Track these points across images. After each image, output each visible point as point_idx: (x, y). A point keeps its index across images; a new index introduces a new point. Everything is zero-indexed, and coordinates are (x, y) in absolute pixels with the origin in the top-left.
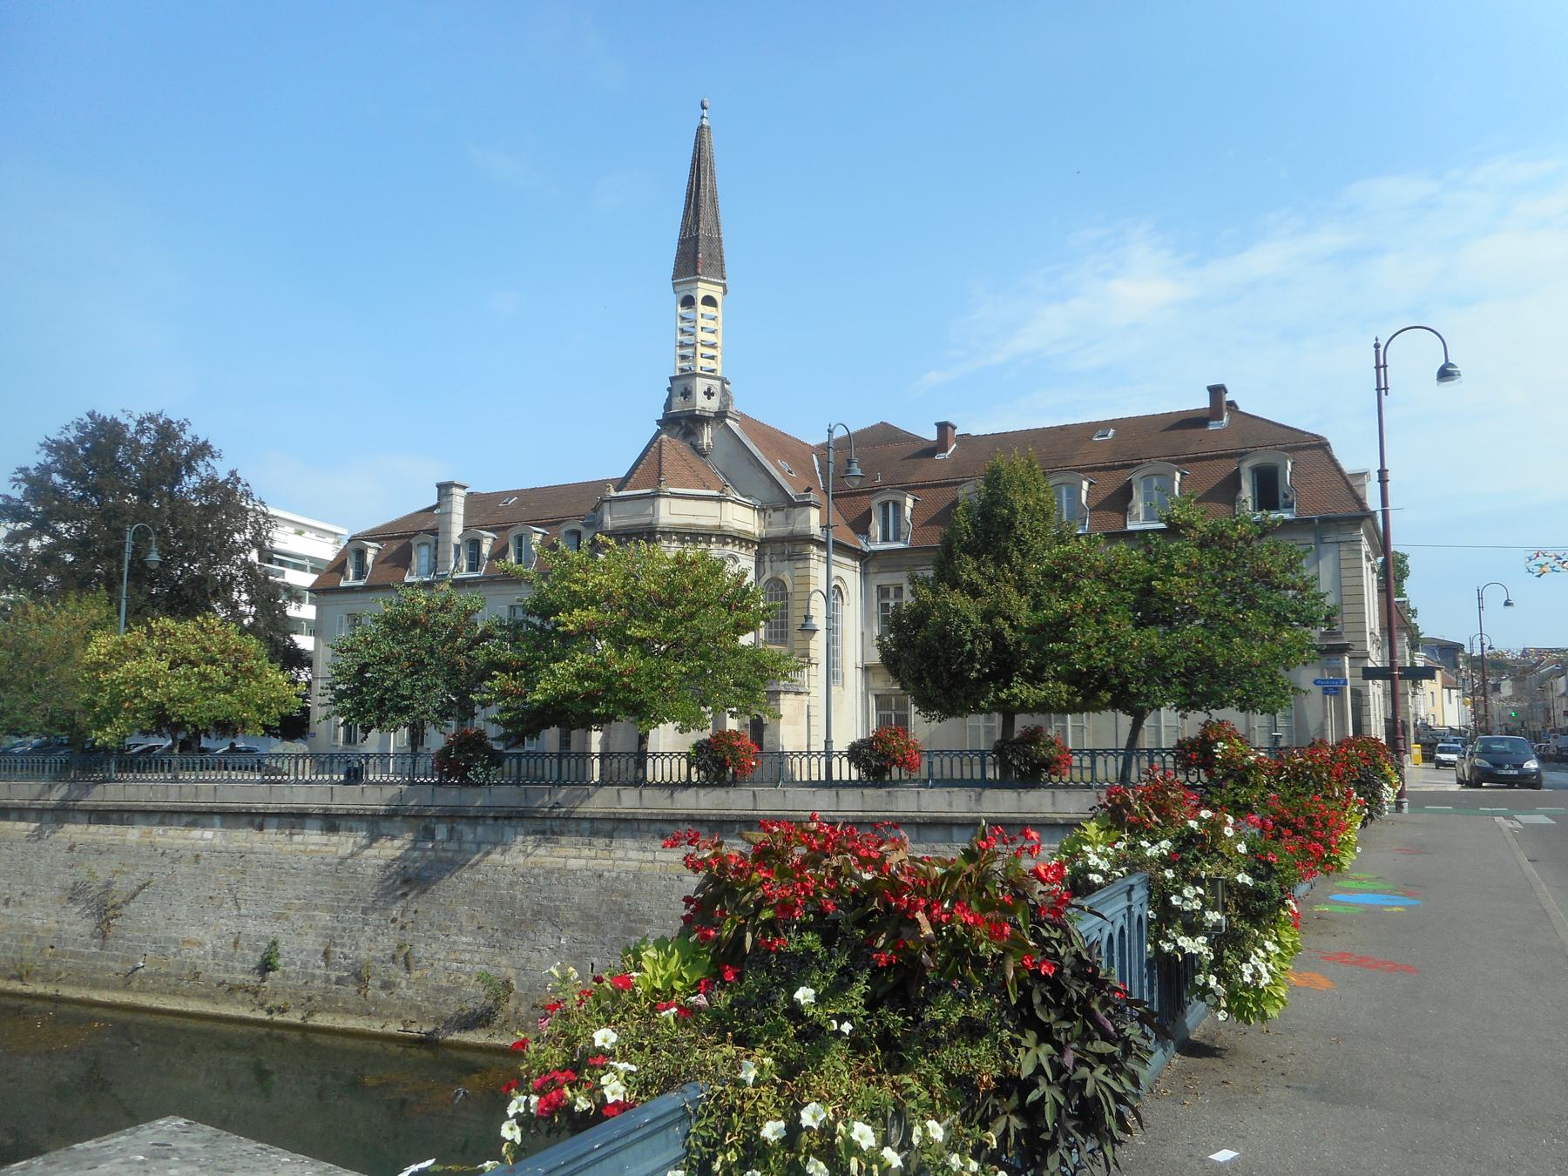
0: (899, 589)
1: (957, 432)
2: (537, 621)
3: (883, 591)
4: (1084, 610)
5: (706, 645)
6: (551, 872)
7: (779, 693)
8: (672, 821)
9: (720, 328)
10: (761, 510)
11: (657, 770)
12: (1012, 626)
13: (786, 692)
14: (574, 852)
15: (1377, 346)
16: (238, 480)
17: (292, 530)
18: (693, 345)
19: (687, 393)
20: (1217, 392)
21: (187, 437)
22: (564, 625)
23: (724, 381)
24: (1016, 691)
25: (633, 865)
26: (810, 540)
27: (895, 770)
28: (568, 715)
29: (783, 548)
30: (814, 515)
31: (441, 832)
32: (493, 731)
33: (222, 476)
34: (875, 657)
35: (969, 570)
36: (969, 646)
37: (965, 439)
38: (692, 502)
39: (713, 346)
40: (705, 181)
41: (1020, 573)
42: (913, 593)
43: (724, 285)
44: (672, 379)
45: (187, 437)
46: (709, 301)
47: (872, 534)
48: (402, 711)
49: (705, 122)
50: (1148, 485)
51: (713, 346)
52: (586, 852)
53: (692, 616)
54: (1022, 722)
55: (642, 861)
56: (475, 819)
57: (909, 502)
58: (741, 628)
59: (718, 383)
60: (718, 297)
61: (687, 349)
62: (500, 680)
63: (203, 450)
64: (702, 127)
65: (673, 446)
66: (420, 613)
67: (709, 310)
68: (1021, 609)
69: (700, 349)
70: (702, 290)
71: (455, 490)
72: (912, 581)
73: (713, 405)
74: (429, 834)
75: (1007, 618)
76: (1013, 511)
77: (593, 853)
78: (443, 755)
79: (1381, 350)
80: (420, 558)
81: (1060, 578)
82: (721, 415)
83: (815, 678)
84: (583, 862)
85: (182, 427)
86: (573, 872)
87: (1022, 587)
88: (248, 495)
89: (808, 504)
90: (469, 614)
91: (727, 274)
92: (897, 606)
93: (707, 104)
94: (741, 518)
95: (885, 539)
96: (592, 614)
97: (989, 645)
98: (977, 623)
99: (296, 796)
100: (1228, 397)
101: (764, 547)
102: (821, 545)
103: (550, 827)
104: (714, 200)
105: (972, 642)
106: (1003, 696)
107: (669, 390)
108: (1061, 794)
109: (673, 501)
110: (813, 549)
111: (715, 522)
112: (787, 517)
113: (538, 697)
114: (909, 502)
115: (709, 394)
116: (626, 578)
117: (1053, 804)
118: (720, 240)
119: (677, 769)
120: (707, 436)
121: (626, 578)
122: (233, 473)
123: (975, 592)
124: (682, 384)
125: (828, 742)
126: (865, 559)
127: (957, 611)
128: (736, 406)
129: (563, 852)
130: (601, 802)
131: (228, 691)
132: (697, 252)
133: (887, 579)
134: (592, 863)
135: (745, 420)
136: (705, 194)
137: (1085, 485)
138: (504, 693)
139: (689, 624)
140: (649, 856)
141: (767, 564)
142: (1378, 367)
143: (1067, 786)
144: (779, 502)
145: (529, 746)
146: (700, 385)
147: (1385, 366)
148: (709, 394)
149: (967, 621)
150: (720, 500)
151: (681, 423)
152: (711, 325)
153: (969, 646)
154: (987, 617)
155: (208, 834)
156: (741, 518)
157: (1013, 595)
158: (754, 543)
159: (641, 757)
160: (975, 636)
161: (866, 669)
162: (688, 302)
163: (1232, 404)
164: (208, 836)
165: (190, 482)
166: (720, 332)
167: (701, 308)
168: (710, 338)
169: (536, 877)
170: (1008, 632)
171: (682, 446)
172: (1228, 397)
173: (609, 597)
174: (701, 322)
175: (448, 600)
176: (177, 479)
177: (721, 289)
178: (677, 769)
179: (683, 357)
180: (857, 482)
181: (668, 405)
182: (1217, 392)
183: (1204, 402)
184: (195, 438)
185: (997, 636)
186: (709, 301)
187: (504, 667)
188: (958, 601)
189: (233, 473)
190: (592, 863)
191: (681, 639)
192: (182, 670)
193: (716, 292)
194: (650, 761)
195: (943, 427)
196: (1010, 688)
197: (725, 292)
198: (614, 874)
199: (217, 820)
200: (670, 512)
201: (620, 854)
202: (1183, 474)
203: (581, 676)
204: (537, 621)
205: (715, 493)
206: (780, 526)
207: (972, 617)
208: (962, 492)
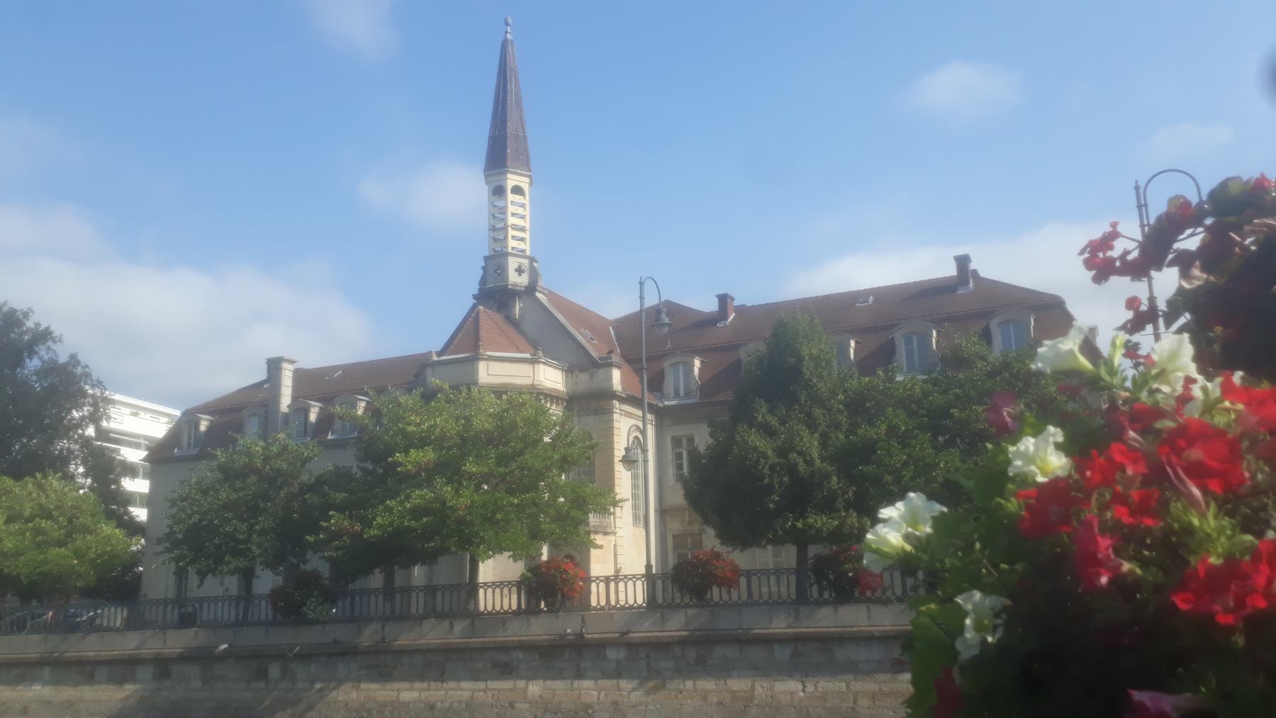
0: (691, 439)
1: (736, 303)
2: (369, 466)
3: (677, 442)
4: (886, 435)
5: (534, 479)
6: (384, 705)
7: (589, 533)
8: (505, 648)
9: (527, 213)
10: (569, 371)
11: (487, 601)
12: (805, 461)
13: (596, 532)
14: (406, 685)
15: (1137, 188)
16: (78, 363)
17: (126, 411)
18: (505, 228)
19: (501, 271)
20: (962, 262)
21: (30, 324)
22: (400, 464)
23: (532, 260)
24: (811, 520)
25: (465, 695)
26: (613, 395)
27: (715, 590)
28: (397, 550)
29: (591, 403)
30: (616, 375)
31: (274, 671)
32: (324, 569)
33: (63, 359)
34: (677, 497)
35: (762, 413)
36: (766, 481)
37: (741, 310)
38: (507, 365)
39: (523, 229)
40: (511, 86)
41: (809, 415)
42: (712, 435)
43: (530, 177)
44: (486, 259)
45: (30, 324)
46: (517, 190)
47: (665, 390)
48: (236, 553)
49: (509, 36)
50: (908, 342)
51: (523, 229)
52: (418, 685)
53: (521, 453)
54: (813, 551)
55: (474, 691)
56: (307, 656)
57: (697, 363)
58: (565, 464)
59: (526, 262)
60: (526, 187)
61: (498, 229)
62: (336, 520)
63: (44, 336)
64: (505, 42)
65: (489, 319)
66: (258, 462)
67: (517, 198)
68: (811, 444)
69: (511, 232)
70: (512, 180)
71: (285, 365)
72: (711, 425)
73: (523, 280)
74: (262, 674)
75: (801, 453)
76: (800, 359)
77: (425, 685)
78: (276, 596)
79: (1141, 191)
80: (253, 426)
81: (859, 407)
82: (531, 289)
83: (623, 519)
84: (415, 695)
85: (26, 315)
86: (406, 704)
87: (811, 424)
88: (87, 375)
89: (611, 365)
90: (305, 461)
91: (532, 167)
92: (693, 453)
93: (510, 21)
94: (551, 377)
95: (677, 395)
96: (428, 456)
97: (786, 479)
98: (773, 459)
99: (128, 644)
100: (972, 266)
101: (573, 401)
102: (623, 400)
103: (384, 663)
104: (519, 103)
105: (771, 477)
106: (800, 525)
107: (484, 268)
108: (876, 609)
109: (492, 364)
110: (616, 404)
111: (528, 382)
112: (592, 377)
113: (374, 532)
114: (697, 363)
115: (520, 271)
116: (457, 419)
117: (869, 618)
118: (525, 137)
119: (510, 601)
120: (518, 307)
121: (457, 419)
122: (73, 356)
123: (769, 432)
124: (495, 262)
125: (649, 567)
126: (662, 415)
127: (755, 448)
128: (541, 283)
129: (396, 685)
130: (432, 634)
131: (60, 544)
132: (505, 148)
133: (680, 431)
134: (424, 695)
135: (552, 296)
136: (511, 99)
137: (853, 343)
138: (337, 535)
139: (519, 459)
140: (482, 685)
141: (575, 419)
142: (1140, 207)
143: (879, 601)
144: (579, 362)
145: (357, 585)
146: (513, 263)
147: (1146, 205)
148: (520, 271)
149: (766, 457)
150: (533, 362)
151: (495, 294)
152: (520, 211)
153: (766, 481)
154: (782, 453)
155: (37, 687)
156: (551, 377)
157: (805, 433)
158: (562, 399)
159: (472, 588)
160: (772, 468)
161: (663, 512)
162: (499, 191)
163: (975, 272)
164: (37, 691)
165: (33, 364)
166: (528, 218)
167: (511, 197)
168: (520, 222)
169: (369, 711)
170: (802, 467)
171: (497, 317)
172: (972, 266)
173: (443, 437)
174: (511, 209)
175: (285, 448)
176: (19, 363)
177: (527, 180)
178: (510, 601)
179: (495, 240)
180: (666, 329)
181: (483, 281)
182: (962, 262)
183: (950, 271)
184: (38, 325)
185: (792, 470)
186: (517, 190)
187: (340, 508)
188: (756, 440)
189: (73, 356)
190: (424, 695)
191: (511, 472)
192: (16, 526)
193: (523, 182)
194: (481, 591)
195: (724, 300)
196: (805, 518)
197: (531, 184)
198: (447, 705)
199: (47, 672)
200: (491, 373)
201: (452, 684)
202: (938, 332)
203: (417, 513)
204: (369, 466)
205: (528, 356)
206: (584, 382)
207: (770, 452)
208: (742, 354)
